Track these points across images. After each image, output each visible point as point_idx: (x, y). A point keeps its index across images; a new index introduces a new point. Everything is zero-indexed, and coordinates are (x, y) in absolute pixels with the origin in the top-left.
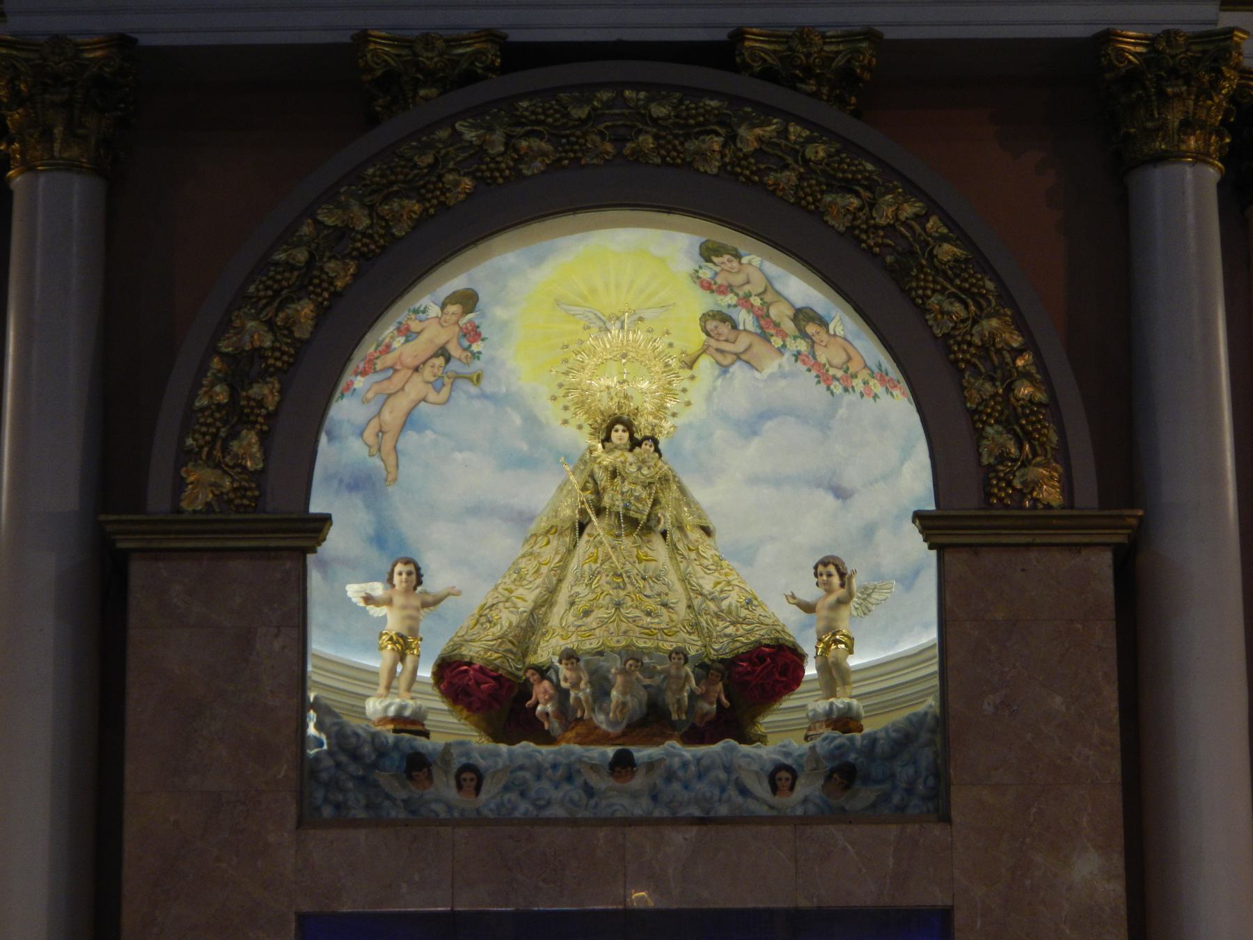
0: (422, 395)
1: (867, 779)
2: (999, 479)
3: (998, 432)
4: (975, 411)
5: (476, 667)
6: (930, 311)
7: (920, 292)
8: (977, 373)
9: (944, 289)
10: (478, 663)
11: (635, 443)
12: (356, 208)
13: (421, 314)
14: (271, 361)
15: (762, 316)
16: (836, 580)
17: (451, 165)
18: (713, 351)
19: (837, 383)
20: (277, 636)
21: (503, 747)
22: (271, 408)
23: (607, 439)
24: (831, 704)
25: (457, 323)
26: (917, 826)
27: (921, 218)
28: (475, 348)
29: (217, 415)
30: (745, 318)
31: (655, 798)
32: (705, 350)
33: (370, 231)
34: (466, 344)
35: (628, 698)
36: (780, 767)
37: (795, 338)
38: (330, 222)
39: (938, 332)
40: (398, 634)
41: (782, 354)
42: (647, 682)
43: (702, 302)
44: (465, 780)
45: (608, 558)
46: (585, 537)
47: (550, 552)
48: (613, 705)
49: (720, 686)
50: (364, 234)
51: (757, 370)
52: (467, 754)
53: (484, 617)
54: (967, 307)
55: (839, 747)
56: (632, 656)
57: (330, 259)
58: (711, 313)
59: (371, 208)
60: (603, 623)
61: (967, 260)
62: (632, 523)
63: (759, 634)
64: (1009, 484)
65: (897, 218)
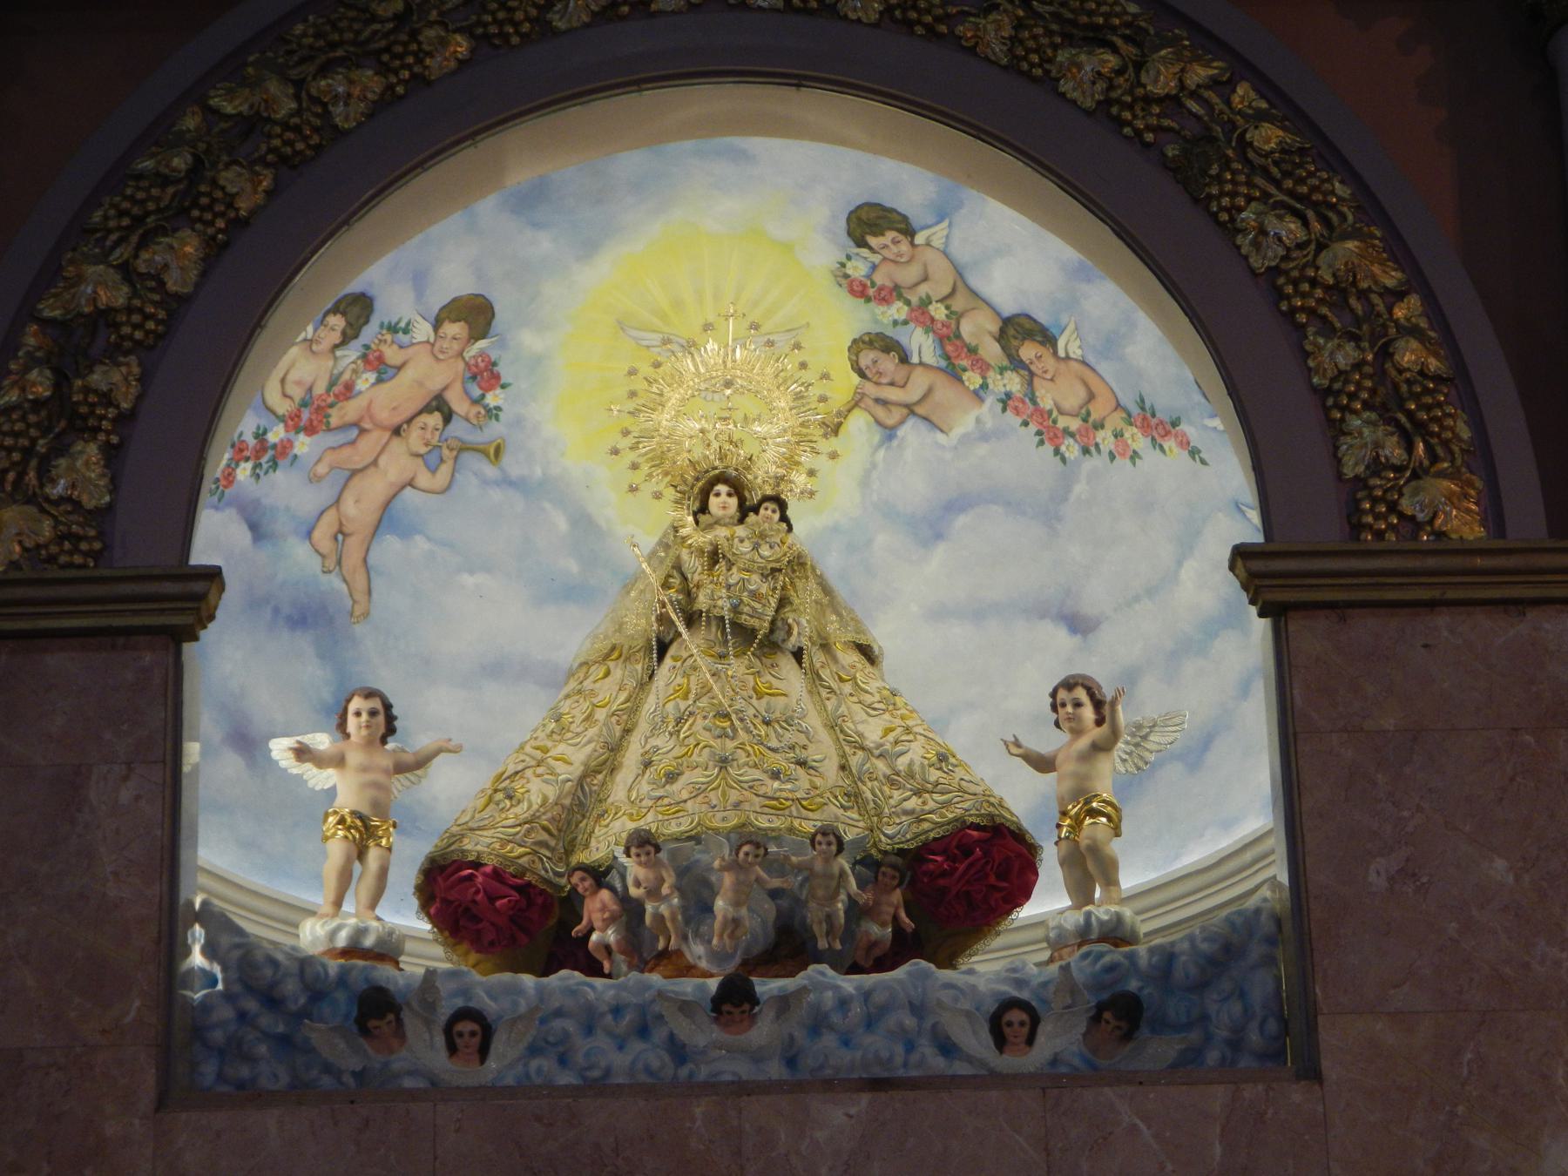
0: (407, 476)
1: (1162, 1025)
2: (1375, 501)
3: (1368, 422)
4: (1328, 391)
5: (488, 869)
6: (1244, 231)
7: (1226, 201)
8: (1328, 330)
9: (1266, 195)
10: (491, 862)
11: (745, 510)
12: (274, 87)
13: (400, 335)
14: (126, 330)
15: (948, 338)
16: (1088, 713)
17: (434, 15)
18: (871, 403)
19: (1071, 441)
20: (126, 778)
21: (528, 980)
22: (125, 405)
23: (704, 509)
24: (1088, 915)
25: (460, 354)
26: (1260, 1087)
27: (1222, 86)
28: (492, 399)
29: (32, 418)
30: (921, 344)
31: (791, 1062)
32: (856, 403)
33: (296, 120)
34: (476, 392)
35: (744, 911)
36: (1010, 1004)
37: (1002, 370)
38: (229, 109)
39: (1256, 262)
40: (353, 813)
41: (982, 400)
42: (776, 883)
43: (854, 319)
44: (461, 1035)
45: (706, 690)
46: (668, 661)
47: (611, 688)
48: (717, 925)
49: (897, 896)
50: (286, 126)
51: (942, 431)
52: (465, 992)
53: (504, 790)
54: (1306, 223)
55: (1112, 968)
56: (751, 841)
57: (227, 166)
58: (867, 339)
59: (299, 84)
60: (698, 791)
61: (1302, 151)
62: (744, 634)
63: (961, 808)
64: (1393, 507)
65: (1182, 85)
